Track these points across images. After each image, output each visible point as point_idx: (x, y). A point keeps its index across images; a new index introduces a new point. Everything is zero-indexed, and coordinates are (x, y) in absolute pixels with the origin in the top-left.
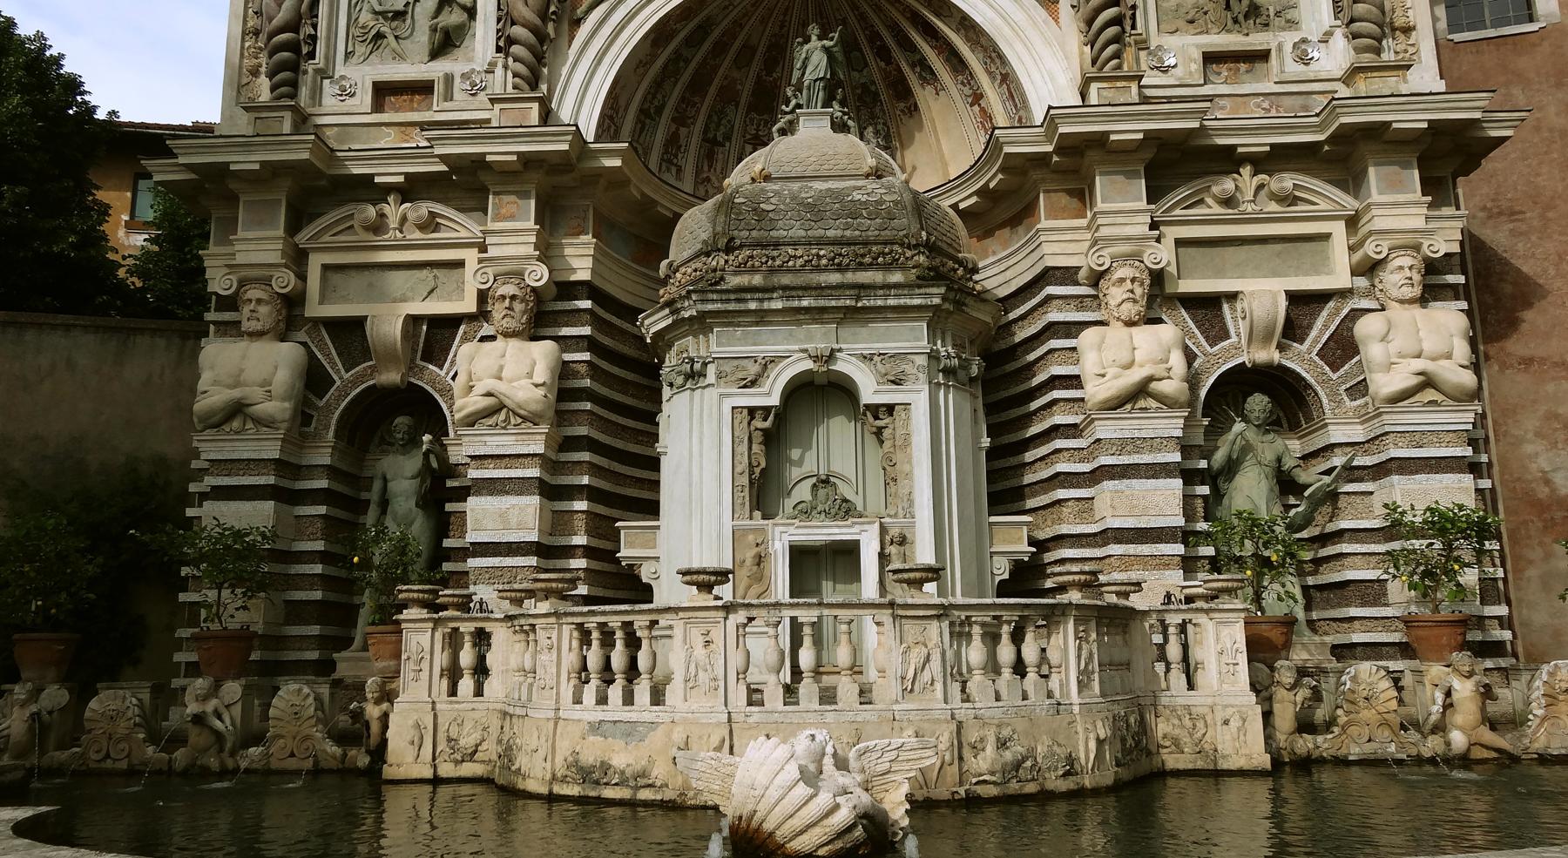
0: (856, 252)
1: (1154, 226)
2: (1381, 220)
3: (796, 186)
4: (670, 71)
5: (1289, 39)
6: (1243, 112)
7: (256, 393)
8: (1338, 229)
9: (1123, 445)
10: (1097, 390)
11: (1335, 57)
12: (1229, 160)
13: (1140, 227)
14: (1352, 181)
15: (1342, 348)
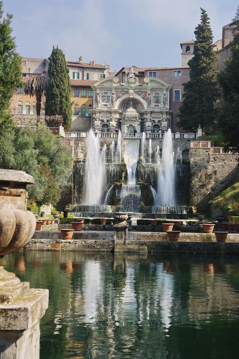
0: (133, 118)
1: (151, 116)
2: (163, 117)
3: (130, 113)
4: (122, 103)
5: (160, 104)
6: (157, 110)
7: (98, 124)
8: (162, 117)
9: (148, 129)
10: (146, 126)
11: (163, 106)
12: (155, 112)
13: (150, 116)
14: (162, 114)
15: (161, 124)
